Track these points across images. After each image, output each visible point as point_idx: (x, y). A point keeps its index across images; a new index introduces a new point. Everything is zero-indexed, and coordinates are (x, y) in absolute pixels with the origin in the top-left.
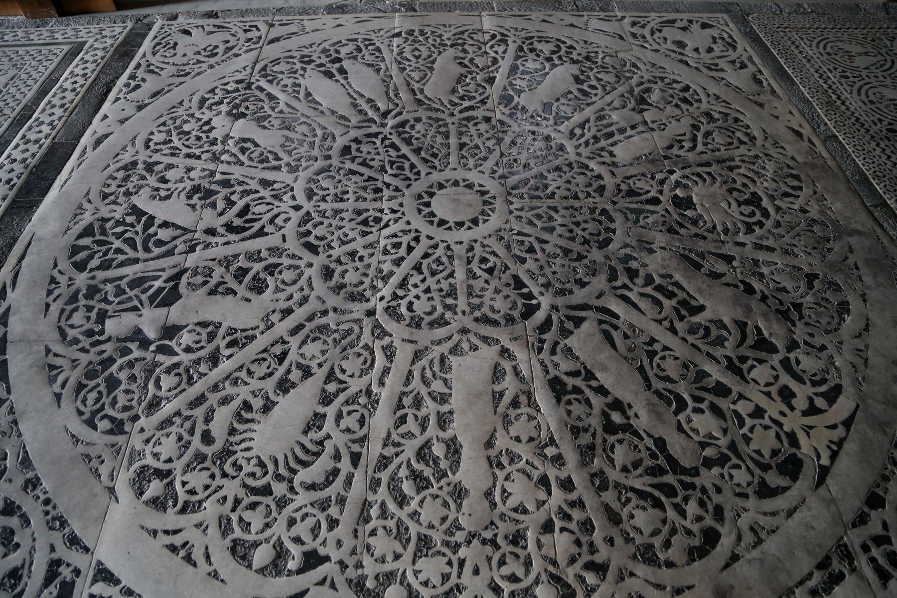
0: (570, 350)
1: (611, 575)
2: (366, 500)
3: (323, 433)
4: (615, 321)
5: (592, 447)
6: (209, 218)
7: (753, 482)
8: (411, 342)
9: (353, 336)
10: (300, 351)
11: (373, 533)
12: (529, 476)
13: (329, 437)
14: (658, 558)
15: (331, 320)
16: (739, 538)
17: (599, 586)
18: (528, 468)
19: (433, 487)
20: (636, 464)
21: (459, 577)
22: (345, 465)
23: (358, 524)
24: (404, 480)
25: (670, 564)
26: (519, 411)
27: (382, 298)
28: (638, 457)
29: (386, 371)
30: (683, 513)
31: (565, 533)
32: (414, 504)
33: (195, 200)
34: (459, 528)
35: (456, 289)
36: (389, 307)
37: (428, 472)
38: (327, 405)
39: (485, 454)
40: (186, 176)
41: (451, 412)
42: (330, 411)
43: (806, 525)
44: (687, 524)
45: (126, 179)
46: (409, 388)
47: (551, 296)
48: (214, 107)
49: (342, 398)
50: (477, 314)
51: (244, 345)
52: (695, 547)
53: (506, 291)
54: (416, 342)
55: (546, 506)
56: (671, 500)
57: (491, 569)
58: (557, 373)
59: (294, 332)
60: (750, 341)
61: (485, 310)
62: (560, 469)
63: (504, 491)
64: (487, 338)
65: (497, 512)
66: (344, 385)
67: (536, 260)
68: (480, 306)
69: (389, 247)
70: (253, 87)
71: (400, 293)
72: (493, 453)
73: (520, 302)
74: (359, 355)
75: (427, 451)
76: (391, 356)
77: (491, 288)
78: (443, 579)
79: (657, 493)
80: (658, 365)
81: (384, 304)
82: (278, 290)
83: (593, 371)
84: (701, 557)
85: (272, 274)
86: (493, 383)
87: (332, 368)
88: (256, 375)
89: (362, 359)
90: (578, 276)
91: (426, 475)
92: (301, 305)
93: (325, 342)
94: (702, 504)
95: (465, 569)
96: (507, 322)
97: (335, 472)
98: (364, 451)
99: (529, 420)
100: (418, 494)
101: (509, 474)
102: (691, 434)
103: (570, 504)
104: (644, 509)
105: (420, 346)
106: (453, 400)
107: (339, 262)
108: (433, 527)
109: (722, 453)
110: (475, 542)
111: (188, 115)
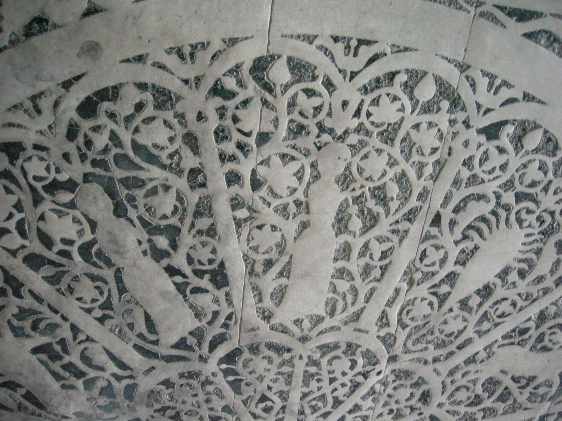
0: (198, 315)
1: (209, 83)
2: (434, 182)
3: (461, 246)
4: (140, 342)
5: (198, 214)
7: (25, 160)
8: (360, 330)
9: (414, 337)
10: (465, 324)
11: (434, 151)
12: (271, 190)
13: (457, 243)
14: (154, 95)
15: (431, 353)
16: (56, 104)
17: (224, 75)
18: (269, 199)
19: (369, 189)
20: (153, 192)
21: (363, 101)
22: (447, 215)
23: (446, 160)
24: (395, 197)
25: (142, 87)
26: (267, 256)
27: (379, 373)
28: (149, 200)
29: (390, 303)
30: (114, 136)
31: (246, 130)
32: (391, 173)
34: (352, 147)
35: (303, 381)
36: (374, 365)
37: (371, 204)
38: (452, 273)
39: (312, 218)
41: (336, 259)
42: (450, 267)
44: (111, 125)
46: (371, 285)
47: (204, 372)
49: (437, 279)
50: (287, 356)
51: (514, 330)
52: (109, 100)
53: (251, 378)
54: (355, 330)
55: (260, 159)
56: (123, 152)
57: (330, 105)
58: (217, 293)
59: (469, 341)
61: (277, 360)
62: (237, 195)
63: (300, 179)
64: (282, 332)
65: (311, 159)
66: (433, 290)
67: (211, 409)
68: (283, 363)
71: (360, 379)
72: (303, 217)
73: (239, 367)
74: (412, 319)
75: (368, 224)
76: (383, 317)
77: (266, 382)
78: (378, 101)
79: (137, 160)
80: (101, 293)
81: (378, 368)
82: (474, 382)
83: (176, 292)
84: (106, 90)
85: (477, 396)
86: (286, 287)
87: (440, 307)
88: (509, 302)
89: (411, 315)
90: (170, 391)
91: (374, 202)
92: (457, 368)
93: (441, 332)
94: (89, 143)
95: (356, 108)
96: (257, 347)
97: (456, 210)
98: (427, 228)
99: (258, 246)
100: (385, 184)
101: (291, 194)
102: (83, 219)
103: (235, 159)
104: (155, 146)
105: (352, 325)
106: (332, 271)
107: (412, 409)
108: (377, 150)
109: (52, 194)
110: (339, 132)
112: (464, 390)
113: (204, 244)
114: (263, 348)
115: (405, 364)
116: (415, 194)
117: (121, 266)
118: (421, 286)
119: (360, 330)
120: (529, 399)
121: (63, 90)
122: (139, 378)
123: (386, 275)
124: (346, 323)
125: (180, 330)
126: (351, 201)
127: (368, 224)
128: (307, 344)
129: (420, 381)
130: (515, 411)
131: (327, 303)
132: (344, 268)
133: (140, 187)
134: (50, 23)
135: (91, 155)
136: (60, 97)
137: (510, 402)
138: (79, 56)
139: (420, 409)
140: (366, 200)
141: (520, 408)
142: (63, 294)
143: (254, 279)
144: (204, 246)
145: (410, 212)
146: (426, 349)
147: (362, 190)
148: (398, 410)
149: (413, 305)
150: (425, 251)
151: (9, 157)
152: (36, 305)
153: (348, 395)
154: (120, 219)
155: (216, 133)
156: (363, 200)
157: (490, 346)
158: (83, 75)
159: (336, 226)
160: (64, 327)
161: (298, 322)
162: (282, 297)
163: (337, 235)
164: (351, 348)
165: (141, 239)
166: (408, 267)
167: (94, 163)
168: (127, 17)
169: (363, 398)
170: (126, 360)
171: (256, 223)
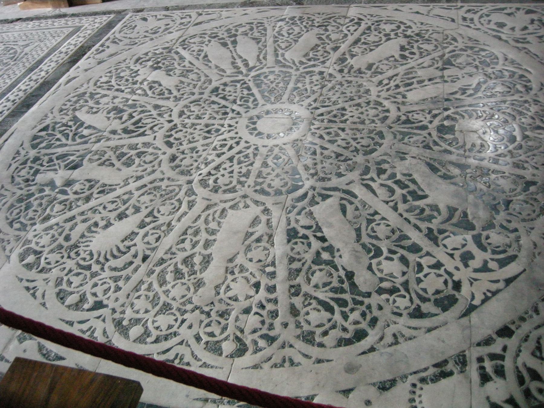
0: (311, 213)
1: (276, 345)
2: (142, 280)
3: (132, 243)
4: (353, 199)
5: (299, 271)
6: (116, 125)
8: (208, 200)
9: (173, 194)
10: (139, 199)
11: (138, 297)
12: (248, 281)
13: (135, 245)
14: (314, 340)
15: (164, 184)
16: (381, 339)
17: (265, 348)
18: (250, 277)
19: (185, 278)
20: (325, 285)
21: (178, 328)
22: (138, 261)
23: (132, 291)
24: (169, 273)
25: (321, 345)
26: (259, 244)
28: (329, 280)
29: (185, 214)
31: (257, 316)
32: (169, 286)
33: (112, 115)
34: (191, 303)
35: (250, 173)
36: (202, 180)
37: (185, 270)
38: (142, 228)
39: (225, 264)
40: (111, 101)
41: (215, 240)
42: (142, 232)
43: (439, 339)
44: (346, 325)
45: (76, 102)
46: (195, 225)
48: (143, 63)
49: (152, 225)
50: (258, 188)
51: (108, 193)
52: (345, 339)
53: (284, 176)
54: (211, 200)
55: (252, 299)
56: (341, 309)
57: (200, 327)
58: (296, 226)
59: (138, 189)
60: (454, 220)
61: (265, 186)
62: (271, 280)
63: (228, 287)
64: (258, 202)
65: (219, 297)
66: (156, 219)
68: (262, 183)
69: (217, 147)
70: (172, 52)
71: (213, 172)
72: (230, 265)
74: (172, 204)
75: (190, 259)
76: (191, 206)
77: (274, 174)
78: (168, 328)
79: (332, 303)
81: (201, 177)
82: (139, 165)
83: (322, 227)
84: (345, 345)
85: (139, 157)
86: (250, 227)
87: (153, 210)
88: (107, 210)
89: (173, 206)
90: (340, 171)
91: (183, 271)
92: (149, 174)
93: (155, 195)
94: (363, 315)
95: (184, 324)
97: (131, 263)
98: (152, 255)
99: (264, 250)
100: (174, 280)
101: (236, 278)
102: (376, 272)
103: (268, 300)
104: (319, 311)
105: (212, 203)
106: (218, 234)
107: (183, 153)
108: (175, 300)
109: (394, 287)
110: (197, 312)
111: (126, 67)
112: (147, 161)
113: (299, 253)
114: (273, 193)
115: (182, 179)
116: (155, 274)
117: (356, 244)
118: (163, 222)
119: (208, 200)
120: (105, 152)
121: (375, 347)
122: (358, 179)
123: (184, 229)
124: (216, 204)
125: (324, 206)
126: (198, 273)
127: (190, 259)
128: (243, 194)
129: (175, 168)
130: (117, 146)
131: (226, 217)
132: (210, 235)
133: (333, 288)
134: (377, 387)
135: (363, 308)
136: (378, 343)
137: (118, 152)
138: (361, 366)
139: (178, 152)
140: (188, 272)
141: (112, 148)
142: (398, 229)
143: (270, 232)
144: (299, 252)
145: (161, 264)
146: (167, 187)
147: (189, 278)
148: (192, 153)
149: (170, 212)
150: (156, 242)
151: (420, 310)
152: (419, 223)
153: (223, 163)
154: (350, 270)
155: (277, 315)
156: (190, 273)
157: (125, 185)
158: (360, 355)
159: (210, 259)
160: (402, 210)
161: (246, 206)
162: (254, 221)
163: (211, 254)
164: (215, 190)
165: (340, 259)
166: (169, 233)
167: (362, 303)
168: (323, 386)
169: (213, 161)
170: (364, 189)
171: (262, 263)
